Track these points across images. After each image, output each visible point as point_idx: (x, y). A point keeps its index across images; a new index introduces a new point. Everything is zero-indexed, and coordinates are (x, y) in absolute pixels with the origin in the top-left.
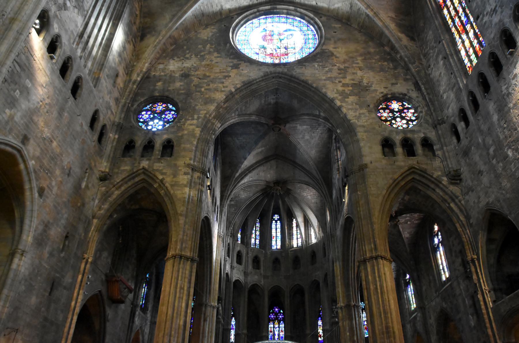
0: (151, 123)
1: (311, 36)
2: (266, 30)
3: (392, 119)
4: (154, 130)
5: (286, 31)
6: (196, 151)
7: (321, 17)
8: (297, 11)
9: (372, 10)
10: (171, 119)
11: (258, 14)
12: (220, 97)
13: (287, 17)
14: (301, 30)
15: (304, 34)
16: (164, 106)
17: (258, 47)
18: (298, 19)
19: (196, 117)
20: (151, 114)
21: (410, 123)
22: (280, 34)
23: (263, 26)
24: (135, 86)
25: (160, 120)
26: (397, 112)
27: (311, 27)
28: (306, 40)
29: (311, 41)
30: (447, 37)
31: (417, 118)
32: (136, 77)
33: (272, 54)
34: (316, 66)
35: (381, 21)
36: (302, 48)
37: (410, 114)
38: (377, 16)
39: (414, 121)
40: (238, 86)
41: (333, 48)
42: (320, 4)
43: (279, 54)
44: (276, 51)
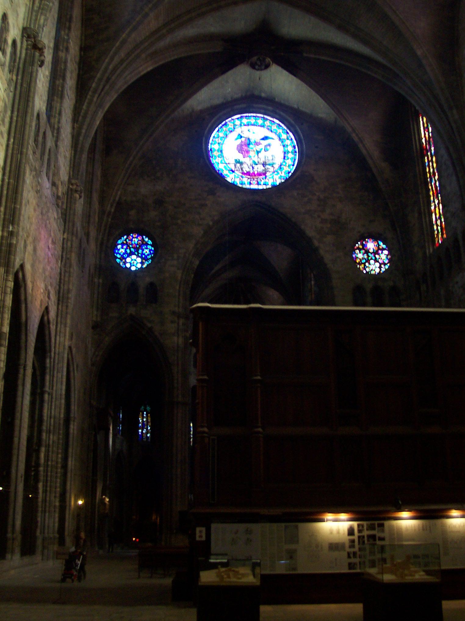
0: (128, 260)
1: (290, 149)
2: (241, 137)
3: (366, 261)
4: (133, 268)
5: (263, 139)
6: (179, 295)
7: (302, 124)
8: (276, 113)
9: (357, 135)
10: (148, 255)
11: (232, 113)
12: (198, 231)
13: (264, 118)
14: (280, 139)
15: (283, 144)
16: (140, 238)
17: (234, 162)
18: (277, 121)
19: (175, 256)
20: (127, 248)
21: (382, 266)
22: (257, 144)
23: (238, 131)
24: (110, 220)
25: (138, 256)
26: (371, 253)
27: (291, 134)
28: (285, 153)
29: (290, 155)
30: (424, 191)
31: (390, 261)
32: (110, 208)
33: (248, 173)
34: (296, 194)
35: (366, 149)
36: (281, 165)
37: (384, 256)
38: (362, 142)
39: (387, 264)
40: (216, 218)
41: (315, 170)
42: (301, 108)
43: (256, 173)
44: (253, 168)
